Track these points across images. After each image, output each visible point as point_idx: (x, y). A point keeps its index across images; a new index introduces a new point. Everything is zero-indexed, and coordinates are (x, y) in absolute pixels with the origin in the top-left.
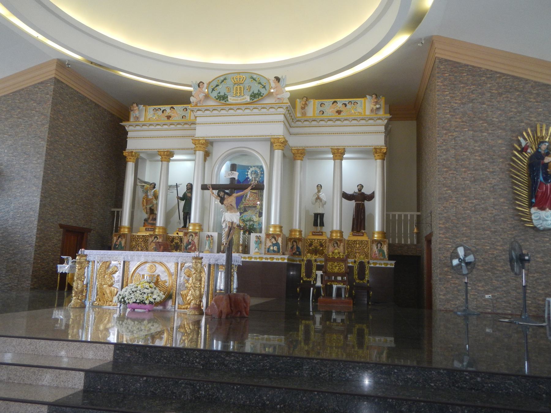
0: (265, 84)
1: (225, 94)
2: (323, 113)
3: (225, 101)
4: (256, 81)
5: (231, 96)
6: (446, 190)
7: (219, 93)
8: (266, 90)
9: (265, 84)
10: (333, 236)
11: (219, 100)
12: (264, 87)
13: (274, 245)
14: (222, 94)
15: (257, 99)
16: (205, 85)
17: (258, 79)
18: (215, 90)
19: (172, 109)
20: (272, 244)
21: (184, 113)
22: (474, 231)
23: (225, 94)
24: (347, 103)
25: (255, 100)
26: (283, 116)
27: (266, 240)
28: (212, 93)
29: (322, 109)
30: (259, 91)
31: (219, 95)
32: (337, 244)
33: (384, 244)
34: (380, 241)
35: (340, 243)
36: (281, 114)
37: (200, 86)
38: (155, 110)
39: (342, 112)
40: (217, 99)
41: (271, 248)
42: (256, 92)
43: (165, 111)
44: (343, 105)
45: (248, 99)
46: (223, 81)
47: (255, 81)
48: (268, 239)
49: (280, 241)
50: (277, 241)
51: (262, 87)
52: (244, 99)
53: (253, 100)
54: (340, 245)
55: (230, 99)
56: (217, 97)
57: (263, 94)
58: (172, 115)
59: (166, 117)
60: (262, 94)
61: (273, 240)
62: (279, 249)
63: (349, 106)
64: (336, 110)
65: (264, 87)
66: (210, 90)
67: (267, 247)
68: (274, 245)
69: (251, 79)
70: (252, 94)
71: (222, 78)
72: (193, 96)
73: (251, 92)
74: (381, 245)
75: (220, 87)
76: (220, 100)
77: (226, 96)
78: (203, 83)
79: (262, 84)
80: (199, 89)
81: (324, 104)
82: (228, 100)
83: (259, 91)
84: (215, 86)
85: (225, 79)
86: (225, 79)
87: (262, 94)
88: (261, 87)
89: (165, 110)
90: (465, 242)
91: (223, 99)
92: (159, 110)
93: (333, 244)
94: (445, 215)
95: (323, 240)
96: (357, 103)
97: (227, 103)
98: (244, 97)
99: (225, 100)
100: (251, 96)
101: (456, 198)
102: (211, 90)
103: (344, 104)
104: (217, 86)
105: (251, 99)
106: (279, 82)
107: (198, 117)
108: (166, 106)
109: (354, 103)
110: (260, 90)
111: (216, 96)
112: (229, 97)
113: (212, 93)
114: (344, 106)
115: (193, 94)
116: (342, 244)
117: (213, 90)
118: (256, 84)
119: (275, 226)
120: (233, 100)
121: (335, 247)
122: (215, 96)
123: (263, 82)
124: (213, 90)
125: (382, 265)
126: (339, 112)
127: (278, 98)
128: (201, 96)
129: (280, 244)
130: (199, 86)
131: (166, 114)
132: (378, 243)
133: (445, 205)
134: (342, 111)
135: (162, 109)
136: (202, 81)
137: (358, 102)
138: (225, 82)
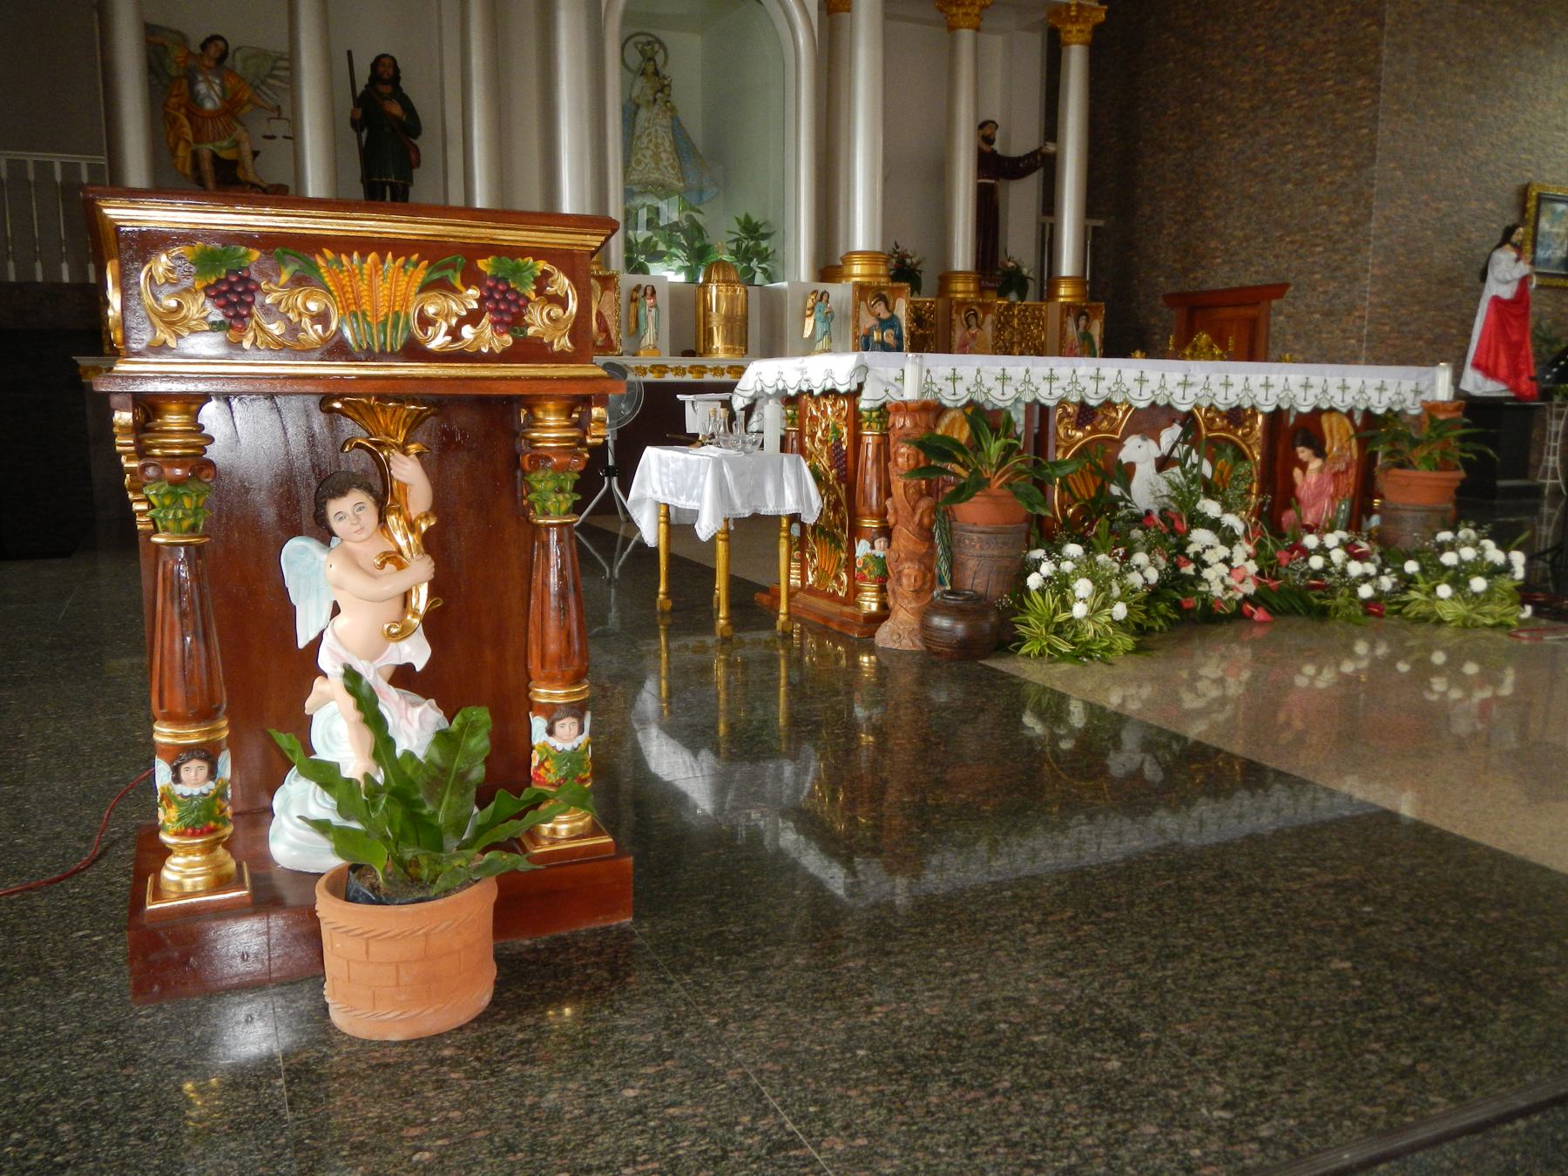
6: (1394, 169)
10: (957, 292)
13: (885, 324)
20: (876, 322)
22: (1434, 288)
27: (857, 307)
32: (975, 315)
33: (1095, 317)
34: (1086, 307)
35: (985, 314)
41: (876, 336)
48: (863, 303)
49: (902, 309)
50: (891, 311)
54: (983, 322)
61: (880, 309)
62: (899, 337)
67: (862, 332)
68: (885, 324)
74: (1088, 320)
90: (1415, 315)
93: (967, 319)
94: (1385, 241)
95: (925, 302)
101: (1409, 193)
116: (989, 318)
119: (870, 256)
121: (969, 327)
125: (684, 374)
129: (904, 324)
132: (1080, 315)
133: (1387, 213)
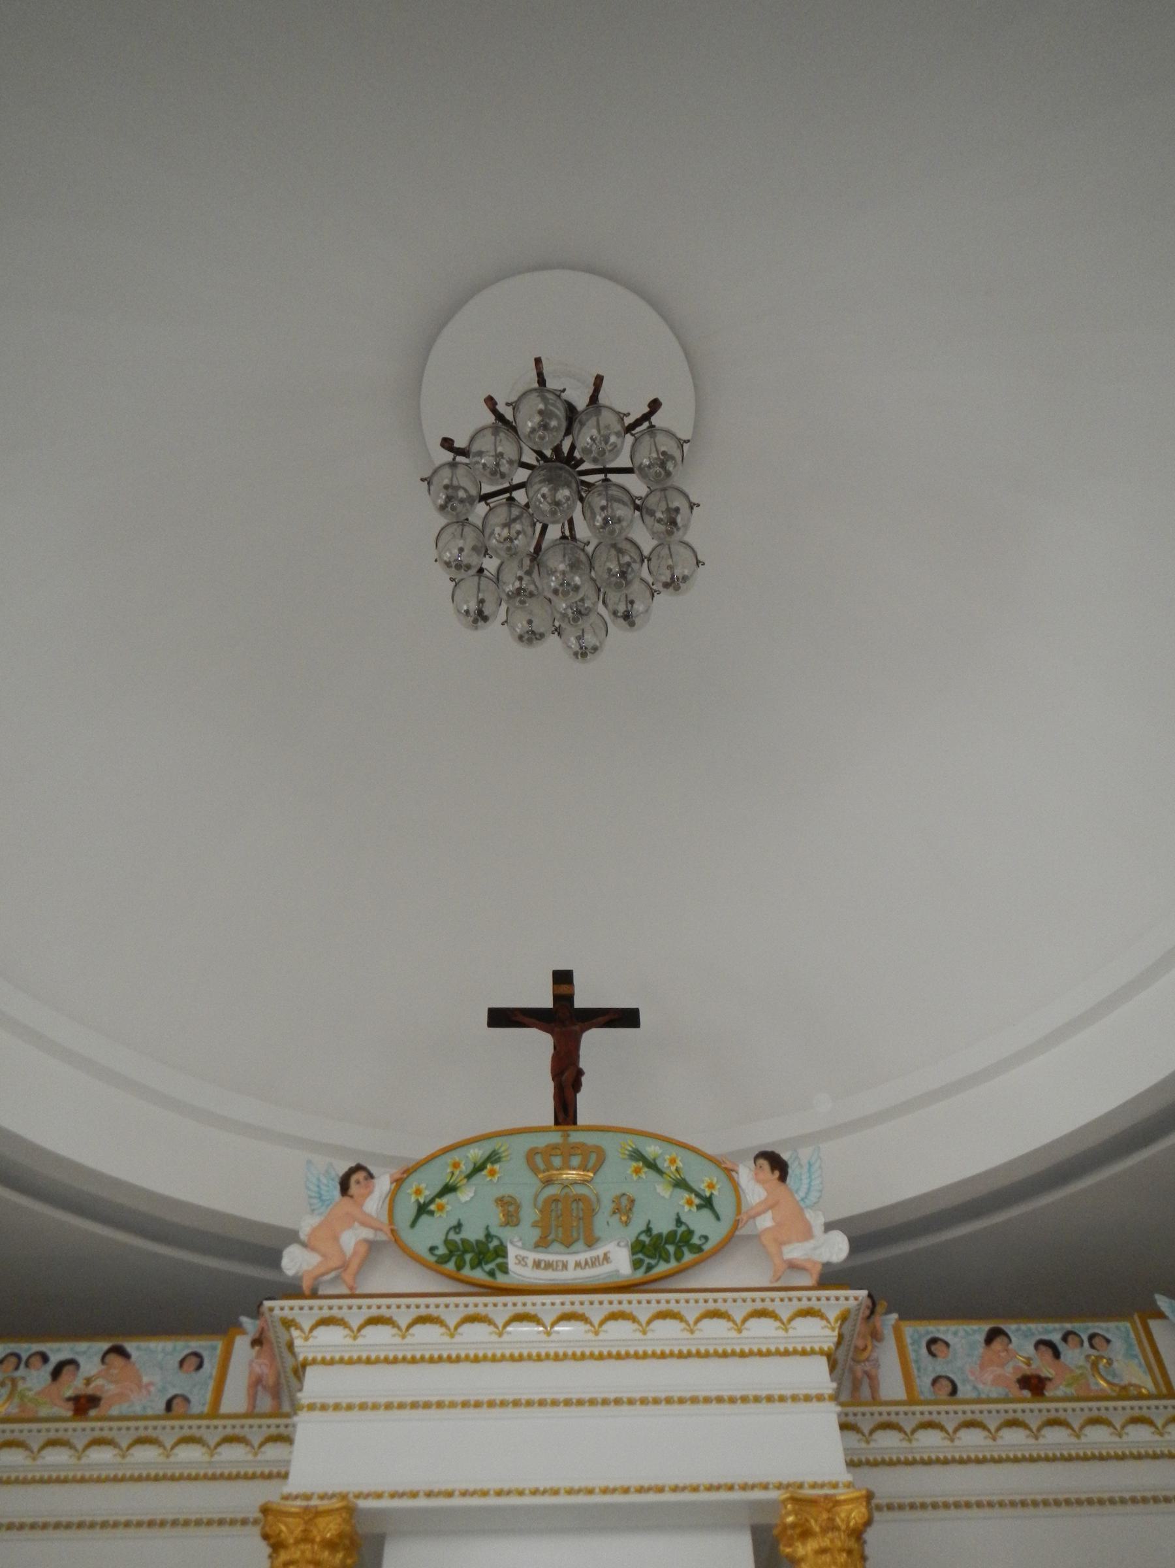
0: (711, 1186)
1: (489, 1236)
2: (954, 1391)
3: (492, 1274)
4: (659, 1171)
5: (523, 1248)
7: (458, 1227)
8: (718, 1218)
9: (711, 1186)
11: (451, 1266)
12: (707, 1203)
14: (473, 1233)
15: (673, 1264)
16: (383, 1184)
17: (673, 1161)
18: (432, 1213)
19: (113, 1358)
21: (180, 1384)
23: (489, 1236)
24: (1056, 1338)
25: (662, 1268)
26: (822, 1363)
28: (413, 1224)
29: (939, 1367)
30: (679, 1222)
31: (453, 1236)
36: (813, 1352)
37: (354, 1189)
38: (14, 1360)
39: (1049, 1386)
40: (443, 1260)
42: (663, 1226)
43: (67, 1370)
44: (1042, 1348)
45: (621, 1263)
46: (478, 1169)
47: (652, 1174)
51: (697, 1201)
52: (594, 1262)
53: (650, 1268)
55: (521, 1261)
56: (442, 1250)
57: (706, 1238)
58: (107, 1387)
59: (71, 1405)
60: (695, 1240)
63: (1073, 1356)
64: (1010, 1371)
65: (707, 1203)
66: (406, 1209)
69: (634, 1164)
70: (643, 1238)
71: (476, 1153)
72: (305, 1245)
73: (638, 1225)
75: (465, 1195)
76: (459, 1267)
77: (495, 1243)
78: (371, 1176)
79: (690, 1189)
80: (346, 1199)
81: (947, 1344)
82: (504, 1269)
83: (679, 1222)
84: (438, 1188)
85: (493, 1158)
86: (493, 1158)
87: (695, 1240)
88: (690, 1203)
89: (72, 1362)
91: (477, 1263)
92: (36, 1361)
96: (1108, 1341)
97: (501, 1280)
98: (599, 1252)
99: (488, 1267)
100: (638, 1248)
102: (413, 1210)
103: (1040, 1343)
104: (448, 1189)
105: (636, 1265)
106: (783, 1178)
107: (314, 1362)
108: (83, 1346)
109: (1092, 1337)
110: (683, 1219)
111: (438, 1241)
112: (512, 1252)
113: (413, 1224)
114: (1048, 1353)
115: (303, 1236)
117: (422, 1209)
118: (663, 1190)
120: (537, 1264)
122: (430, 1244)
123: (703, 1178)
124: (422, 1209)
126: (1034, 1385)
127: (793, 1266)
128: (351, 1239)
130: (344, 1185)
131: (73, 1385)
134: (1050, 1380)
135: (54, 1359)
136: (364, 1163)
137: (1109, 1336)
138: (492, 1173)
